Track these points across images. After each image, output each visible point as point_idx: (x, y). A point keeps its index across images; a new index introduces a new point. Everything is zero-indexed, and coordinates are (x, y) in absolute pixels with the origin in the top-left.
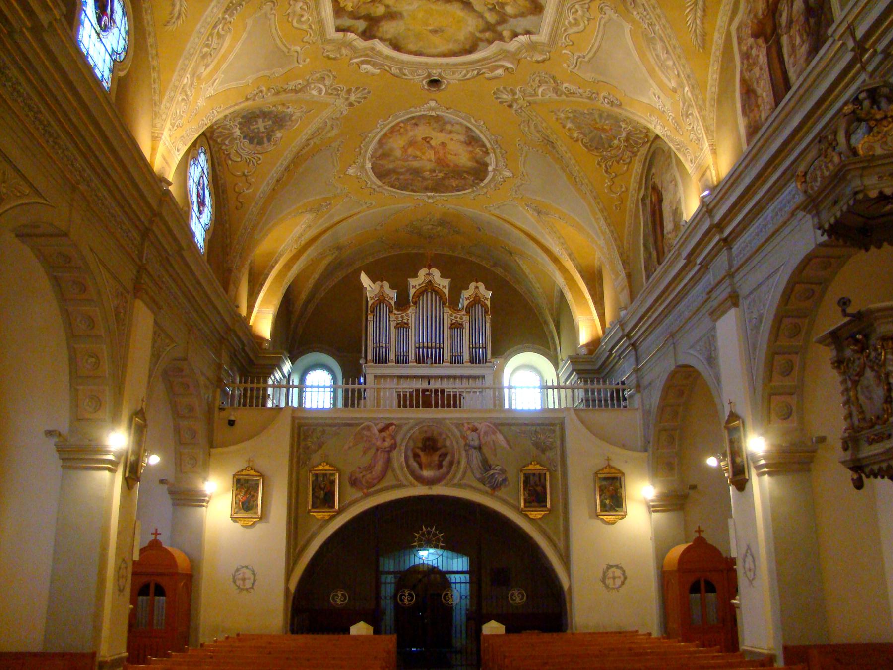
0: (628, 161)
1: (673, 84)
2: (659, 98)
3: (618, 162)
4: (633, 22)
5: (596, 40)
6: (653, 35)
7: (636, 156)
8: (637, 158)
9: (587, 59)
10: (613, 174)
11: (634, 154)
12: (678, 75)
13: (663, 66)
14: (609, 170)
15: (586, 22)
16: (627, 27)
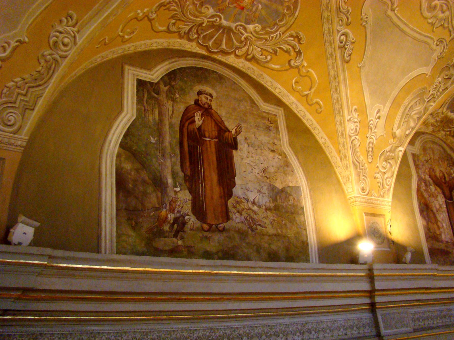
0: (174, 29)
1: (398, 133)
2: (379, 118)
3: (172, 17)
4: (433, 77)
5: (412, 29)
6: (427, 100)
7: (181, 37)
8: (178, 40)
9: (390, 13)
10: (154, 16)
11: (187, 36)
12: (407, 136)
13: (406, 116)
14: (163, 8)
15: (430, 21)
16: (426, 70)
